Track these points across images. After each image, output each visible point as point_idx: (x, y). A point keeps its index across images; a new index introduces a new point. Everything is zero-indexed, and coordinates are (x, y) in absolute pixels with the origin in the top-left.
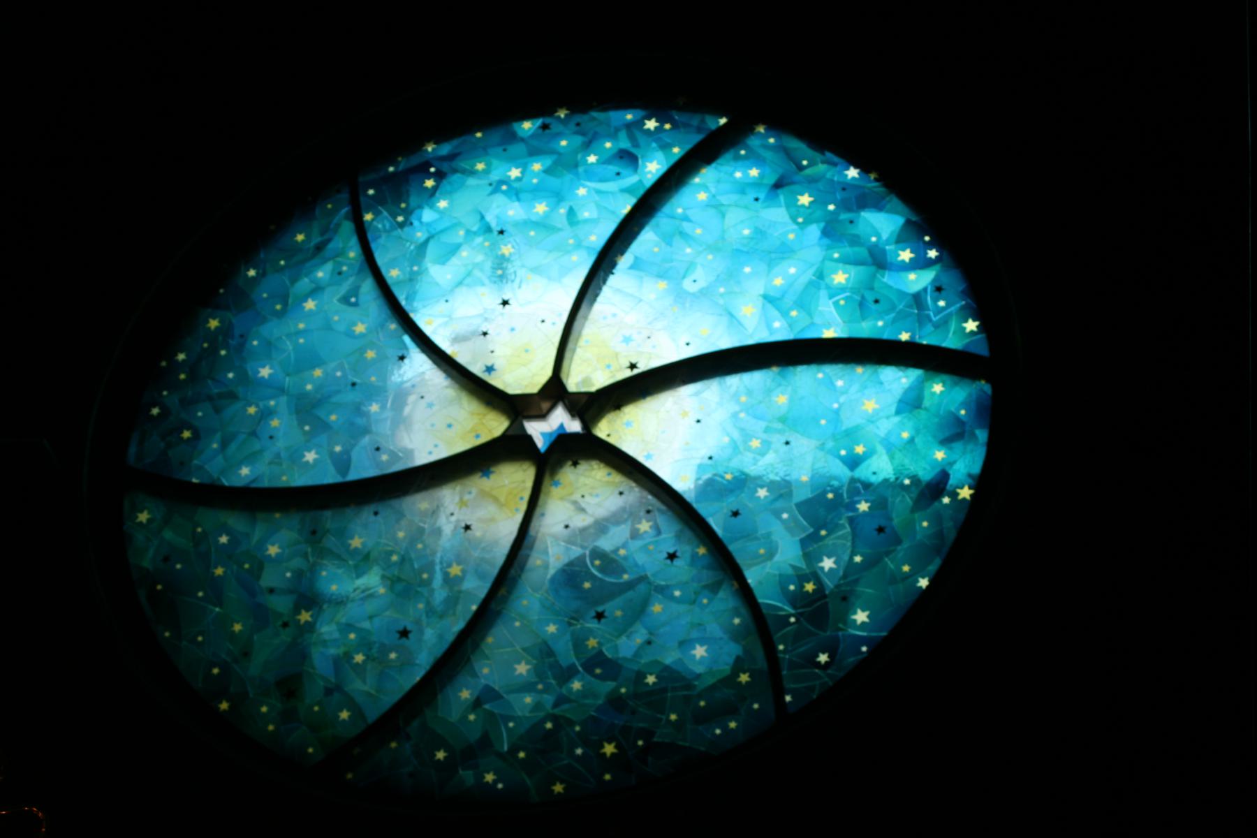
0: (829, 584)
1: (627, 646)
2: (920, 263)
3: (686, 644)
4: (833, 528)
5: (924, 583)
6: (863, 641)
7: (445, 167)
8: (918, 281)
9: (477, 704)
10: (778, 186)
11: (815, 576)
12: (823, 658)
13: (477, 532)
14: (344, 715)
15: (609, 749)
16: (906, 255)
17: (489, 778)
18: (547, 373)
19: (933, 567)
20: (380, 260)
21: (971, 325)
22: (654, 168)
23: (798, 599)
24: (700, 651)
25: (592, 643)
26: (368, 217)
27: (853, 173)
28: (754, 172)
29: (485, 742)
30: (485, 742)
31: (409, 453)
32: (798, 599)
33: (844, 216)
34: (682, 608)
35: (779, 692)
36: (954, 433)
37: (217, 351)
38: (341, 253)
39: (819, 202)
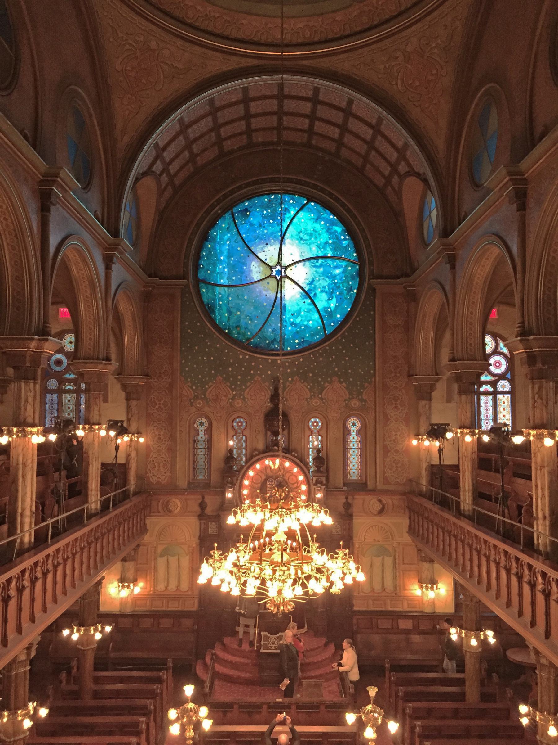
0: (333, 309)
1: (298, 320)
2: (345, 239)
3: (308, 321)
4: (332, 298)
5: (349, 309)
6: (339, 321)
7: (251, 209)
8: (345, 243)
9: (272, 332)
10: (317, 219)
11: (330, 308)
12: (332, 324)
13: (268, 296)
14: (249, 333)
15: (297, 341)
16: (342, 237)
17: (277, 346)
18: (277, 261)
19: (351, 306)
20: (241, 233)
21: (355, 254)
22: (292, 212)
23: (326, 312)
24: (311, 322)
25: (292, 320)
26: (237, 221)
27: (331, 217)
28: (312, 215)
29: (275, 339)
30: (275, 339)
31: (253, 278)
32: (326, 312)
33: (330, 227)
34: (306, 314)
35: (325, 331)
36: (353, 278)
37: (211, 253)
38: (233, 230)
39: (325, 224)
